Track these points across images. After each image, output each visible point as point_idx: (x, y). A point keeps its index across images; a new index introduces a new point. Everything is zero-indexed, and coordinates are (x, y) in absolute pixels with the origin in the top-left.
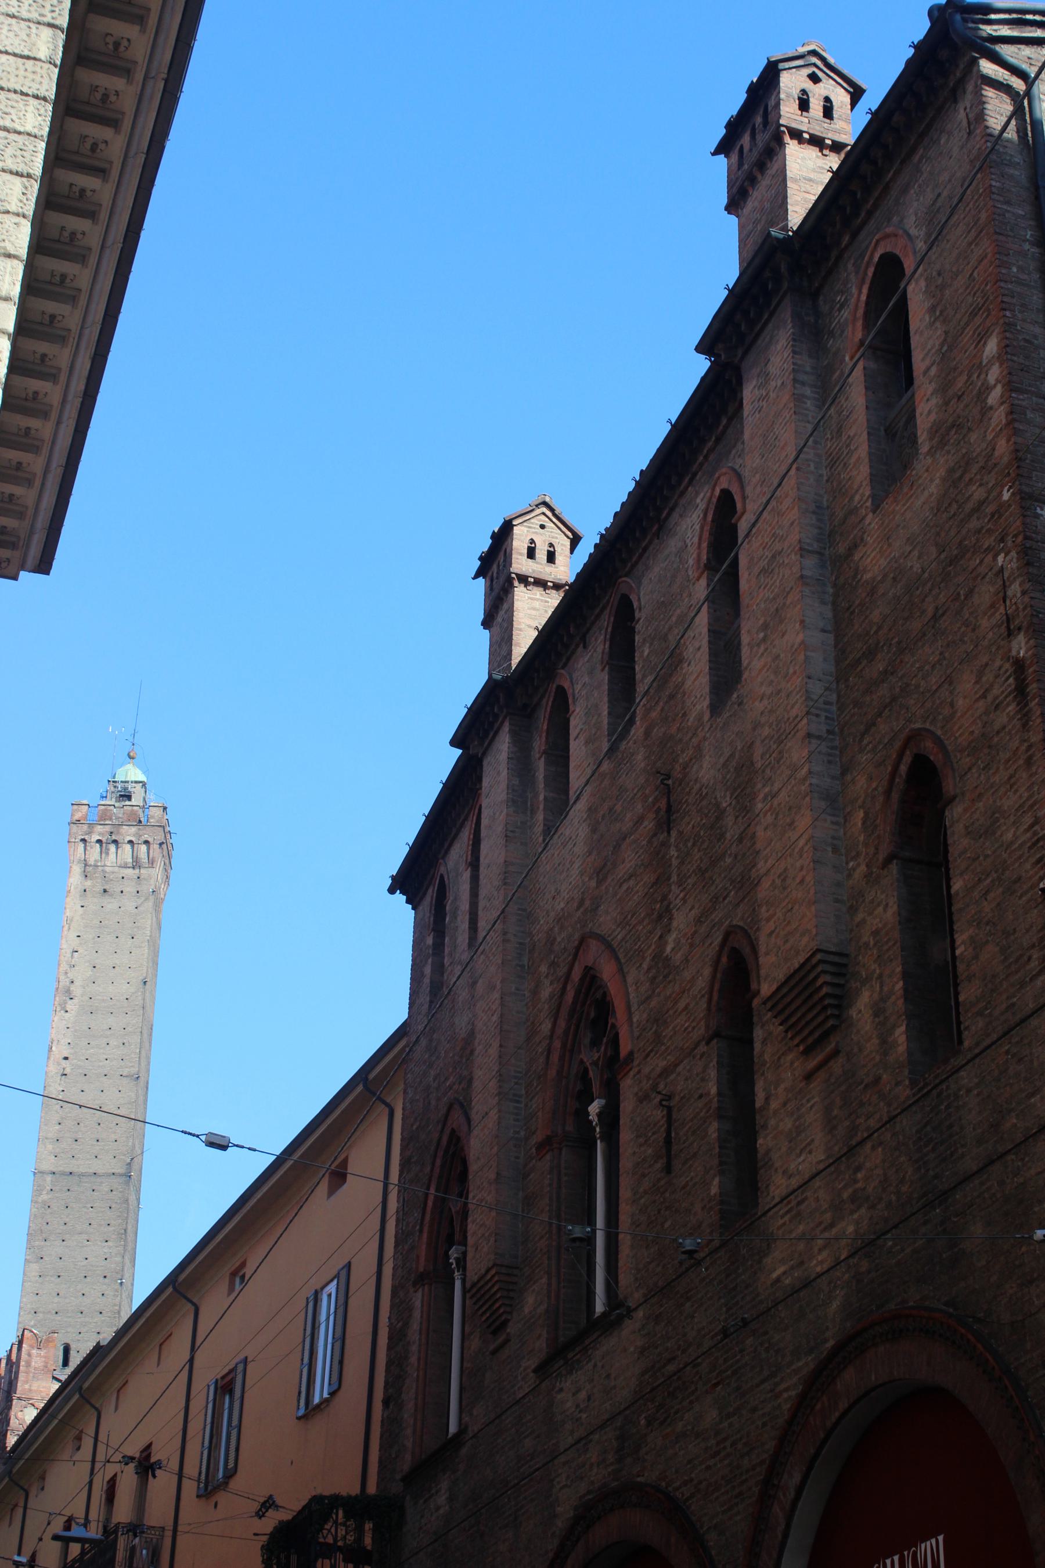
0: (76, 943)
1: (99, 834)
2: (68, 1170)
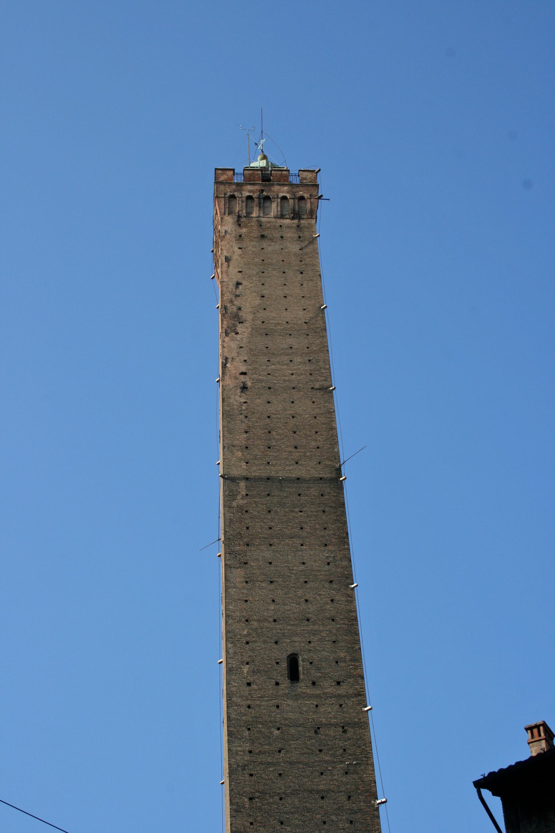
1: (250, 191)
2: (264, 475)
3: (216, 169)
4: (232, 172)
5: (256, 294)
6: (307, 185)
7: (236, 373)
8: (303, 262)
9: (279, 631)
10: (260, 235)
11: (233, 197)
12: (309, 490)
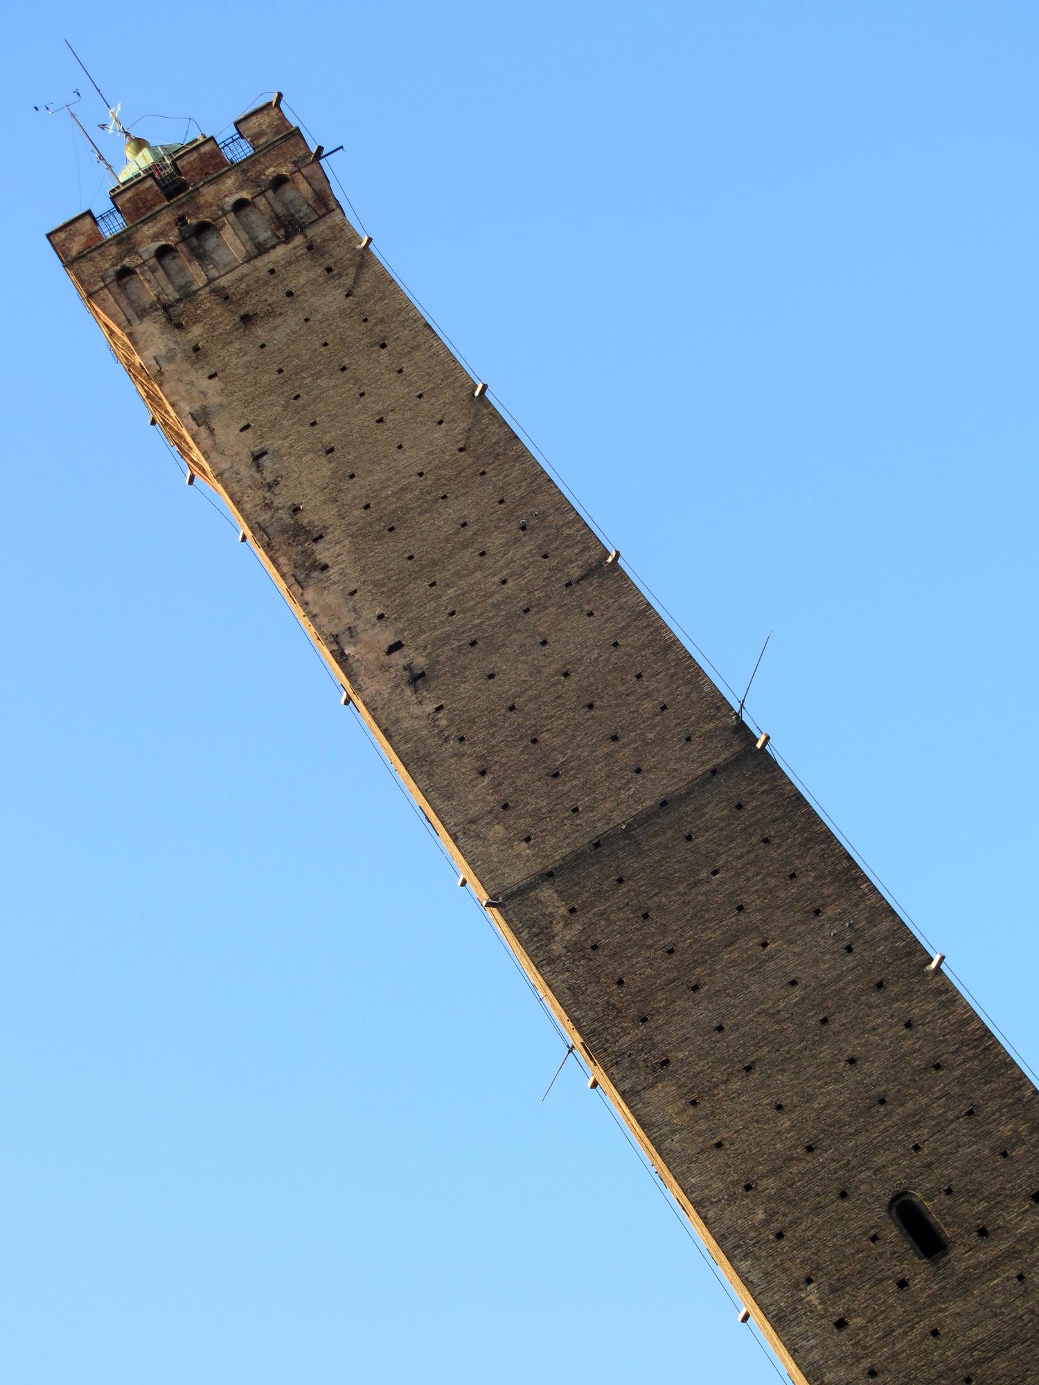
1: (155, 237)
2: (583, 841)
3: (48, 236)
4: (88, 220)
5: (311, 456)
6: (272, 145)
7: (378, 658)
8: (372, 320)
9: (834, 1166)
10: (238, 320)
11: (125, 274)
12: (703, 815)
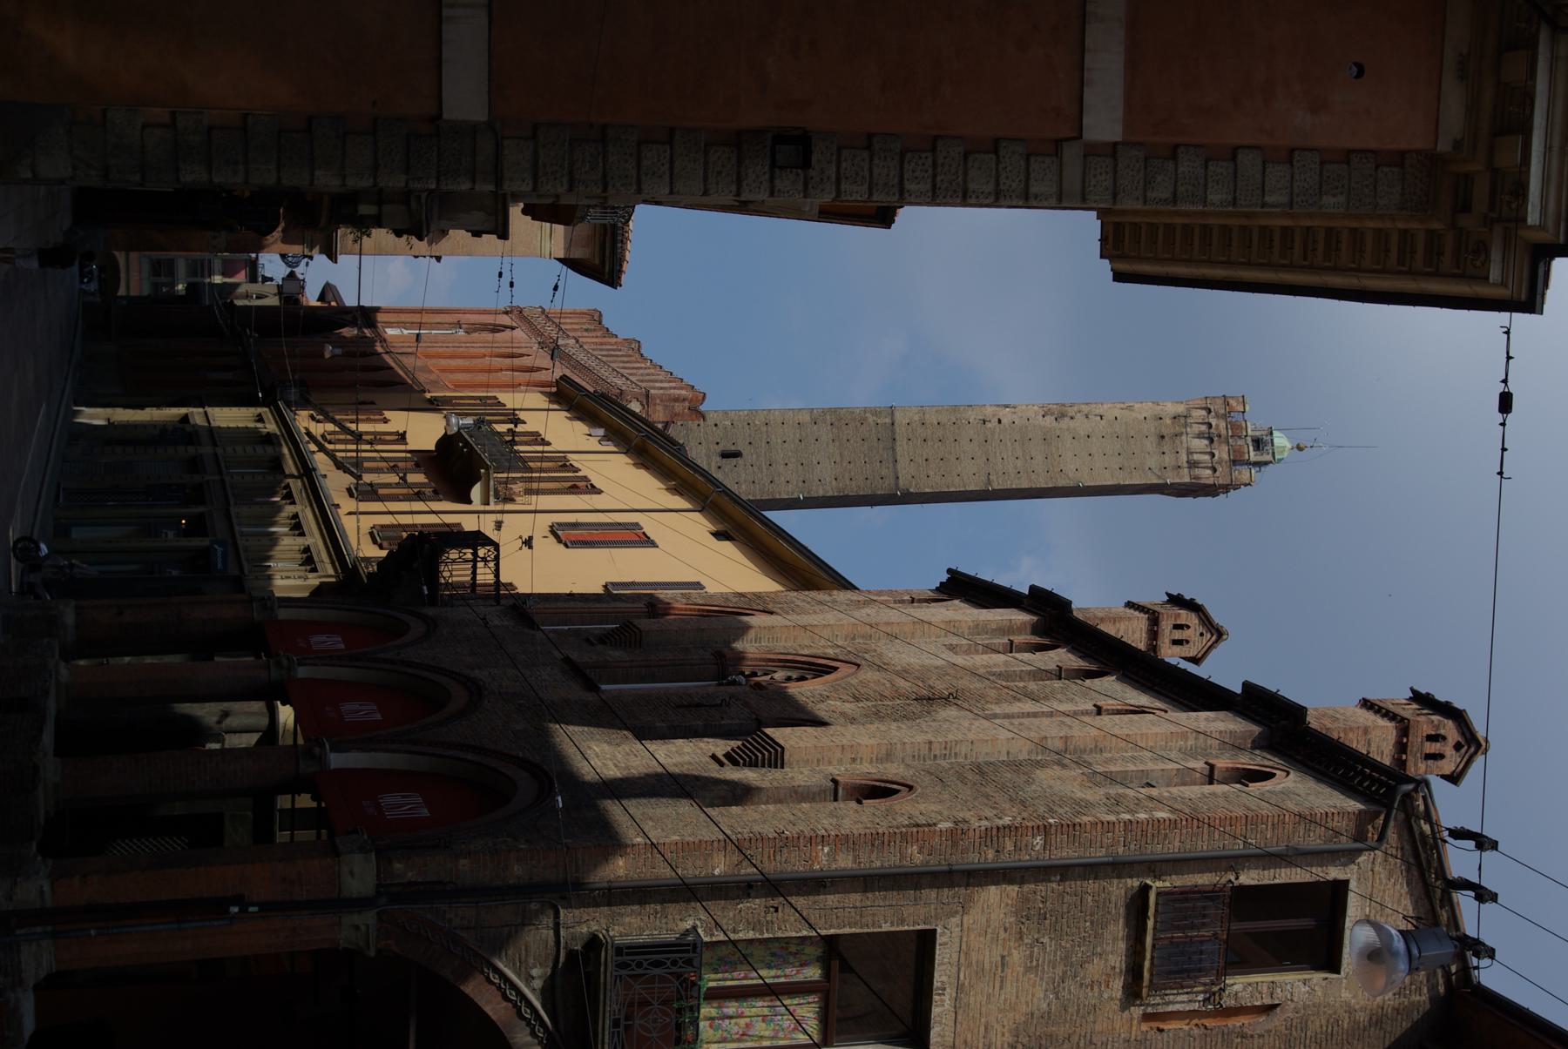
0: (1110, 416)
